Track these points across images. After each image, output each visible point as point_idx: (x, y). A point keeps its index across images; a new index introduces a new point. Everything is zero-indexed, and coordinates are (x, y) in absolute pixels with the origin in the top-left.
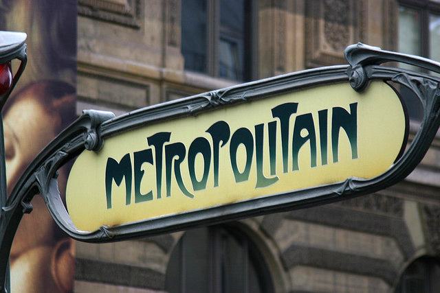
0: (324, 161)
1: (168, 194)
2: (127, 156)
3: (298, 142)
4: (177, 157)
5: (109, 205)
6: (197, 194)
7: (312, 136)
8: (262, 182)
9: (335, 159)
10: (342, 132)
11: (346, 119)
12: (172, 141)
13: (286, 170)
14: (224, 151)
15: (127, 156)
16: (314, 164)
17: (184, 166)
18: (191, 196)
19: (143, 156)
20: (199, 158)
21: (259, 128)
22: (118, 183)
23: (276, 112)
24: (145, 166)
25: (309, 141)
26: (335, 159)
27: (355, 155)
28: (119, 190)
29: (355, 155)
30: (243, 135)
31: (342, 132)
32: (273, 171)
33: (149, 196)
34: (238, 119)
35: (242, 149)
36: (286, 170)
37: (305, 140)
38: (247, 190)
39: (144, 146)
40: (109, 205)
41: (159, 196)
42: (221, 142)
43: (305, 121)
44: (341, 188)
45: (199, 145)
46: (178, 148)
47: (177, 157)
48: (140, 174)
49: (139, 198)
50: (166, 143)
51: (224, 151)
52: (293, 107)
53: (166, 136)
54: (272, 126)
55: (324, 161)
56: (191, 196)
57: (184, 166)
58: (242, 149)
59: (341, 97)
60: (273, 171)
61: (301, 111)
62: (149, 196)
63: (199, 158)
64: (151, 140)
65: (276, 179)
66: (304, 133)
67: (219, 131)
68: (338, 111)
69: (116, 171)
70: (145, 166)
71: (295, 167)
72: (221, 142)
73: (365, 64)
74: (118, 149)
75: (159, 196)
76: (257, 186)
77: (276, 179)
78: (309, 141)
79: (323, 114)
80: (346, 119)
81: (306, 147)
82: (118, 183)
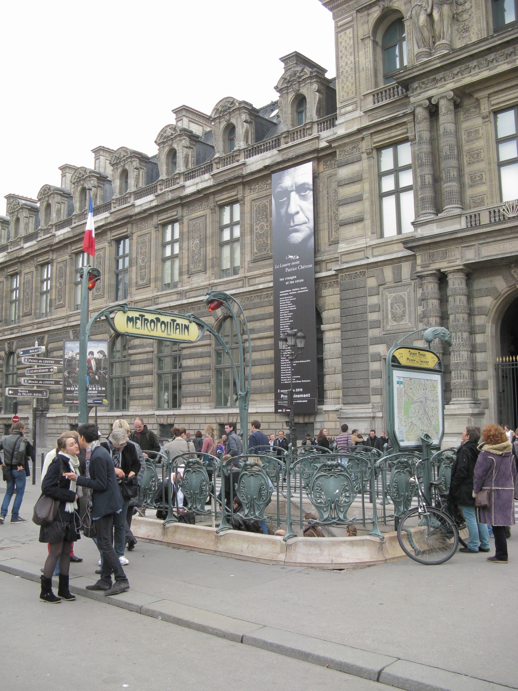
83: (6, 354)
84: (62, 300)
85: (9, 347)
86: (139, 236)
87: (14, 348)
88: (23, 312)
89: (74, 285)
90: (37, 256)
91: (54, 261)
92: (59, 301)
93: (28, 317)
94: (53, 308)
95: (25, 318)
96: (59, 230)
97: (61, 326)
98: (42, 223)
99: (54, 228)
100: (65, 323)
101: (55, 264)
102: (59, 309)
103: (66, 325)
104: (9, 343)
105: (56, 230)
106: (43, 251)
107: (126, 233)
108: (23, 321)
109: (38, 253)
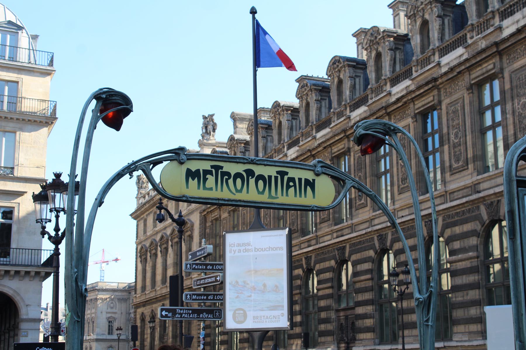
0: (300, 196)
1: (222, 190)
2: (198, 171)
3: (288, 187)
4: (227, 177)
6: (237, 194)
7: (295, 186)
8: (270, 196)
9: (305, 196)
10: (308, 188)
11: (310, 184)
12: (224, 170)
13: (282, 195)
14: (252, 181)
15: (199, 170)
16: (296, 195)
17: (231, 181)
18: (235, 194)
20: (239, 181)
21: (270, 177)
22: (193, 179)
23: (278, 172)
24: (208, 176)
25: (293, 187)
26: (305, 196)
27: (314, 197)
28: (193, 183)
29: (314, 197)
30: (261, 177)
31: (308, 188)
33: (211, 189)
34: (258, 170)
35: (261, 183)
36: (282, 195)
37: (292, 186)
38: (264, 198)
39: (210, 169)
40: (187, 187)
41: (217, 190)
42: (250, 177)
43: (292, 179)
44: (311, 208)
45: (238, 175)
46: (228, 174)
47: (227, 177)
48: (205, 180)
49: (205, 188)
50: (220, 170)
51: (252, 181)
52: (287, 173)
53: (222, 168)
54: (276, 178)
55: (300, 196)
56: (235, 194)
57: (231, 181)
58: (261, 183)
59: (309, 175)
61: (290, 175)
62: (211, 189)
63: (239, 181)
64: (212, 167)
65: (278, 198)
66: (291, 184)
67: (250, 173)
68: (307, 180)
69: (191, 174)
70: (208, 176)
71: (287, 195)
72: (250, 177)
73: (322, 167)
74: (194, 166)
75: (217, 190)
77: (278, 198)
78: (293, 187)
79: (300, 180)
80: (310, 184)
81: (292, 190)
82: (193, 179)
83: (303, 272)
84: (363, 199)
85: (306, 263)
86: (449, 104)
87: (312, 265)
88: (320, 217)
89: (376, 178)
90: (330, 146)
91: (351, 150)
92: (360, 200)
93: (326, 224)
94: (354, 209)
95: (323, 225)
96: (354, 110)
97: (364, 232)
98: (335, 104)
99: (348, 109)
100: (368, 228)
101: (352, 154)
102: (360, 211)
103: (369, 230)
104: (305, 258)
105: (351, 111)
106: (337, 138)
107: (433, 103)
108: (321, 228)
109: (331, 142)
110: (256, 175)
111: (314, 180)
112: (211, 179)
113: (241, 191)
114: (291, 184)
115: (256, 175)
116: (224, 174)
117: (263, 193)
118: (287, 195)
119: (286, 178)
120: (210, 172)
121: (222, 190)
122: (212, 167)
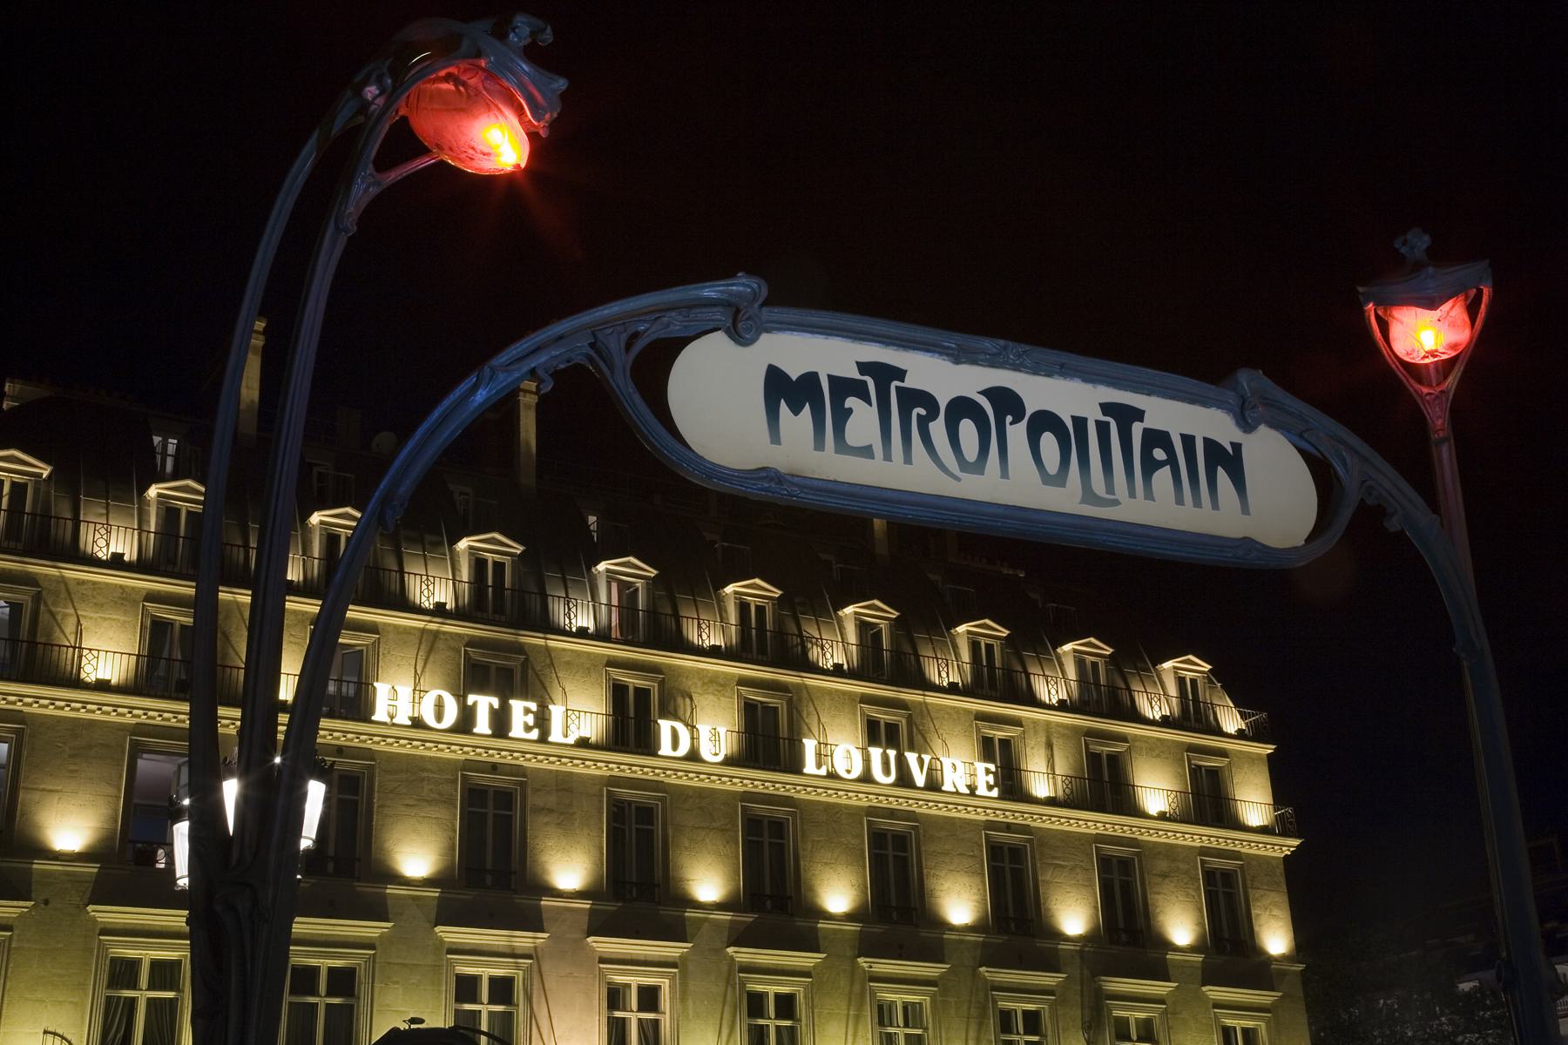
0: (1197, 502)
1: (908, 459)
2: (811, 379)
3: (1150, 466)
4: (923, 412)
5: (775, 436)
7: (1172, 460)
8: (1089, 496)
9: (1215, 506)
10: (1221, 472)
11: (1226, 459)
12: (909, 383)
13: (1132, 494)
14: (1017, 433)
16: (1180, 500)
18: (958, 479)
19: (842, 387)
20: (967, 428)
21: (1080, 423)
22: (796, 410)
23: (1107, 408)
26: (1215, 506)
27: (1245, 509)
28: (797, 424)
29: (1245, 509)
30: (1044, 422)
31: (1221, 472)
32: (1110, 487)
33: (867, 452)
36: (1132, 494)
37: (1161, 464)
40: (775, 436)
41: (888, 457)
42: (1009, 418)
45: (961, 408)
46: (926, 400)
47: (923, 412)
48: (842, 415)
49: (842, 446)
53: (900, 374)
54: (1103, 428)
55: (1197, 502)
56: (958, 479)
57: (938, 428)
58: (1048, 441)
60: (1110, 487)
61: (1151, 422)
62: (867, 452)
63: (967, 428)
65: (1116, 503)
67: (1007, 402)
69: (783, 390)
70: (851, 402)
71: (1149, 494)
72: (1009, 418)
75: (888, 457)
76: (1082, 502)
77: (1116, 503)
79: (1188, 441)
80: (1226, 459)
81: (1163, 476)
82: (796, 410)
110: (1029, 412)
111: (1237, 447)
112: (863, 419)
113: (979, 465)
114: (1159, 454)
115: (1029, 412)
116: (912, 398)
117: (1060, 479)
118: (1149, 494)
119: (1137, 429)
120: (860, 390)
121: (908, 459)
122: (864, 367)
